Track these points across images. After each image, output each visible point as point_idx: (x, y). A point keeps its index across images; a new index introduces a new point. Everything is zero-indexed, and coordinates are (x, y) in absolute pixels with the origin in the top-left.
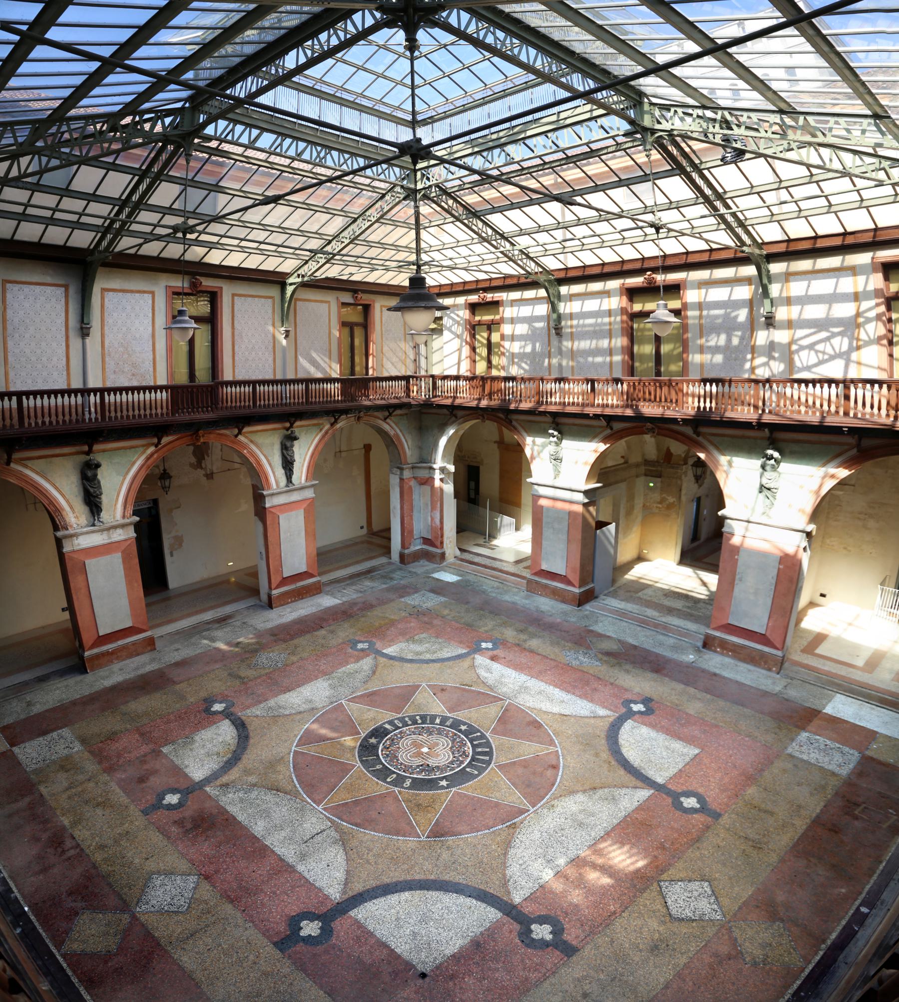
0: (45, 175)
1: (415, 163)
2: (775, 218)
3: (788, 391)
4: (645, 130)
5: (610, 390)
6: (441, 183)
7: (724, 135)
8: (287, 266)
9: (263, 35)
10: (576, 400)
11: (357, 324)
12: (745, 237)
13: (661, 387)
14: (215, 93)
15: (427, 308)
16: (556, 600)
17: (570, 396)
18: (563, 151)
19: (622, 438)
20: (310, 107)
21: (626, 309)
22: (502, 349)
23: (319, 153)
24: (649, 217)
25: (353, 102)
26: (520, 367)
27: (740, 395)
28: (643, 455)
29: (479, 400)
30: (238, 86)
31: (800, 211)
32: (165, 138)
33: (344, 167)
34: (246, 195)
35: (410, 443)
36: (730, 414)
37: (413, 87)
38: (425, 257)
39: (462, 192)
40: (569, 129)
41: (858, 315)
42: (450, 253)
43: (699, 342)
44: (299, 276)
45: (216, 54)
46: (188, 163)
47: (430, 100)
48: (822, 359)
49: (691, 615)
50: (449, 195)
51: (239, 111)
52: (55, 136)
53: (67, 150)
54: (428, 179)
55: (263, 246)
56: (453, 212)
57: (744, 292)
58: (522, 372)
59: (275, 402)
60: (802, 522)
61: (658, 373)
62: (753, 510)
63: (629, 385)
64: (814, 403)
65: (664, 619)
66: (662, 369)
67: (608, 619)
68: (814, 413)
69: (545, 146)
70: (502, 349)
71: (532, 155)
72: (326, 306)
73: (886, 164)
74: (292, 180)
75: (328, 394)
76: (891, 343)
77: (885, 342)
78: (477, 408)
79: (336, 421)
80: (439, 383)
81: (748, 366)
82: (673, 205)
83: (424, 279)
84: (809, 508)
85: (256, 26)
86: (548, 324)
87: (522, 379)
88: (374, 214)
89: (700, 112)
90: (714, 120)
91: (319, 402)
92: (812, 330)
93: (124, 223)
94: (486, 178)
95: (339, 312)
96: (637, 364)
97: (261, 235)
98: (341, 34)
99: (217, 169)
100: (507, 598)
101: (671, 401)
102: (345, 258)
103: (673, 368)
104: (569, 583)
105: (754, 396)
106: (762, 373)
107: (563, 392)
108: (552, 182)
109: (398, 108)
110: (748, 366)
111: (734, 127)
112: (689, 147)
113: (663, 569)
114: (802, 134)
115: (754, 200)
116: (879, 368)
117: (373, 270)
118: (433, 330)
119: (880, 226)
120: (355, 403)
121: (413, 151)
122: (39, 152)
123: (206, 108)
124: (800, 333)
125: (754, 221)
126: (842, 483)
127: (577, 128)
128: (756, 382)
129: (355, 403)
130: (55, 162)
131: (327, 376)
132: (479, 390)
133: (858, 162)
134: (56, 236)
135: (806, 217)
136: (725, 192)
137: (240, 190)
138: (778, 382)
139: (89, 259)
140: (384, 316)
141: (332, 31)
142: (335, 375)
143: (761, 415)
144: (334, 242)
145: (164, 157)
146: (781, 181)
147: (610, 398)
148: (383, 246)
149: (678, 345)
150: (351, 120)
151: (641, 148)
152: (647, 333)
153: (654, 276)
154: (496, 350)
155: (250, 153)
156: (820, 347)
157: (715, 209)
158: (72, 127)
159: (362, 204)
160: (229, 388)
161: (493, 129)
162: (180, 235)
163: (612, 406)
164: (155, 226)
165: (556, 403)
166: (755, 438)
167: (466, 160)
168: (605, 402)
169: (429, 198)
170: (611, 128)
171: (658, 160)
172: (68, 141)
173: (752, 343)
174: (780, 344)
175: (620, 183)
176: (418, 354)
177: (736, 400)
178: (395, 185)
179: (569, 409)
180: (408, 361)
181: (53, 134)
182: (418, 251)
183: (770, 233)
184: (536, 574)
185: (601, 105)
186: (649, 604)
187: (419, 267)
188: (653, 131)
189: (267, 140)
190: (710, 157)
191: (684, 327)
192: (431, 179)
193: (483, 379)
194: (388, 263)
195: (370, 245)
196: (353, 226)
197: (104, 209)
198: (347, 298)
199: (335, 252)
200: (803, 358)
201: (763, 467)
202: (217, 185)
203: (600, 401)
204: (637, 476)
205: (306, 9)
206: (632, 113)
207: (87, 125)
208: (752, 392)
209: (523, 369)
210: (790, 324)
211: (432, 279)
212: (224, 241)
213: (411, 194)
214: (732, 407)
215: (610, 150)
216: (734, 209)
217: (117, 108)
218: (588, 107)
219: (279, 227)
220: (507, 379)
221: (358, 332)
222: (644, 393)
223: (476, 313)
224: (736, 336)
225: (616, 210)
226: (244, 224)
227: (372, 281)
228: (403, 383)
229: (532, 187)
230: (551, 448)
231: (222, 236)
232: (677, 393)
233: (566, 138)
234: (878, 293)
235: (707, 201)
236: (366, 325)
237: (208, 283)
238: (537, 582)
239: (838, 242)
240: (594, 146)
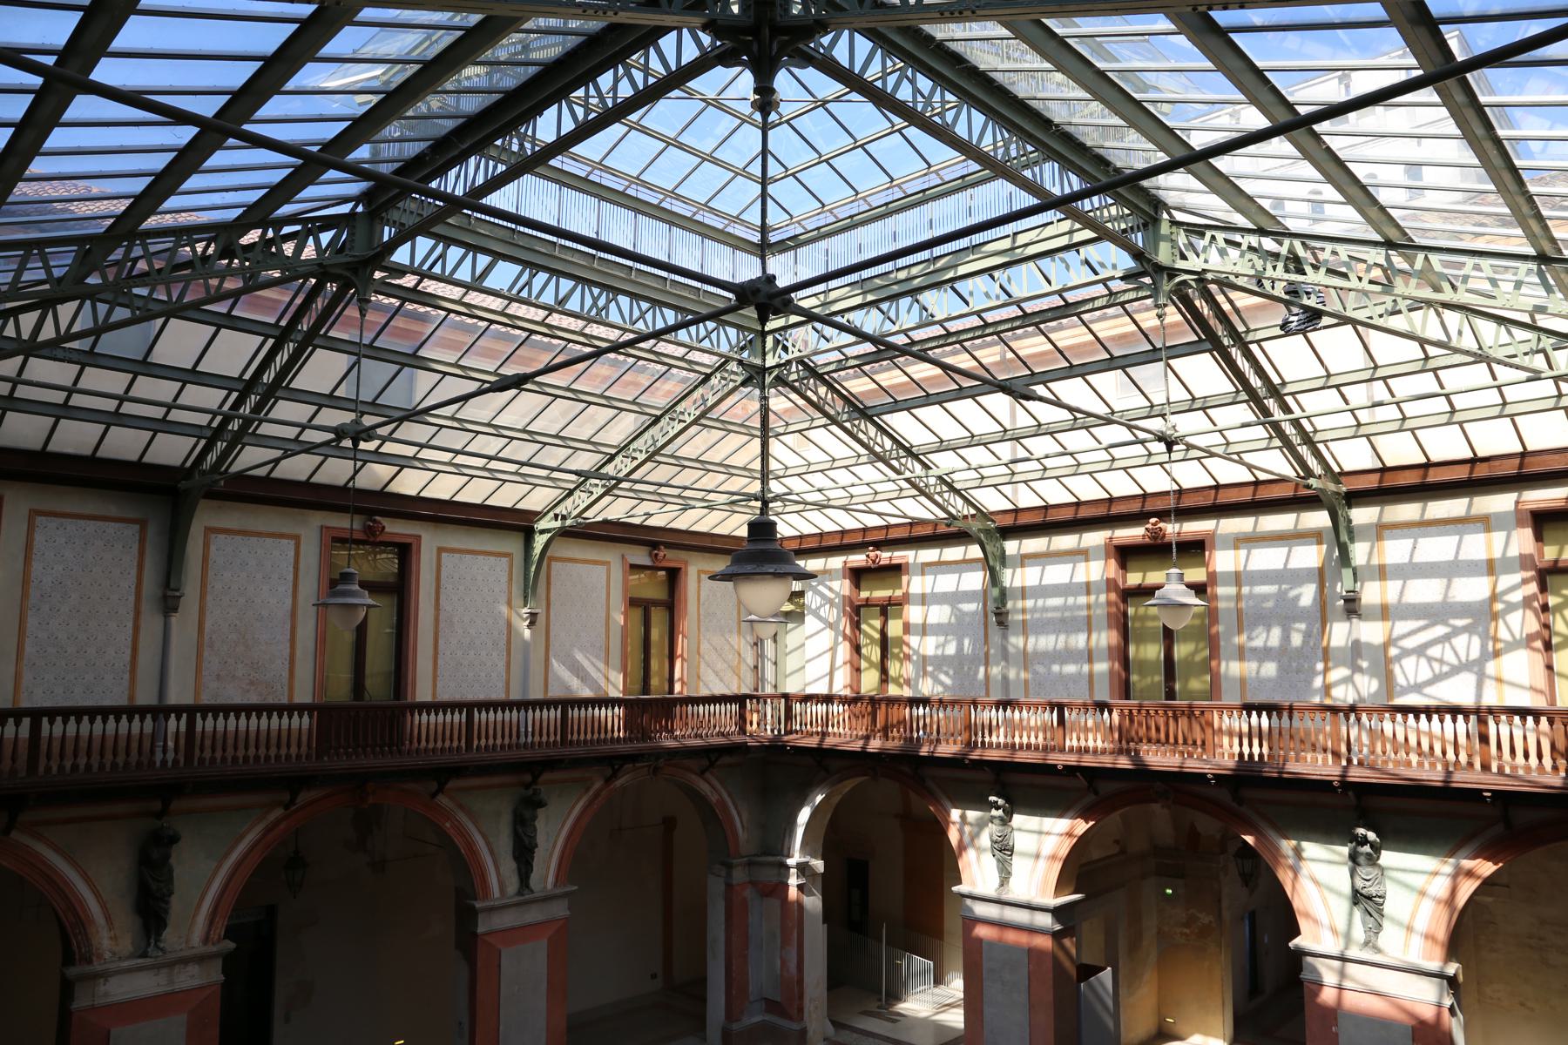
0: (104, 337)
1: (763, 320)
2: (1363, 430)
3: (1388, 726)
4: (1159, 269)
5: (1090, 723)
6: (808, 356)
7: (1291, 283)
8: (537, 500)
9: (497, 76)
10: (1033, 740)
11: (656, 603)
12: (1312, 463)
13: (1176, 719)
14: (408, 187)
15: (778, 576)
17: (1021, 734)
18: (1018, 303)
20: (581, 215)
21: (1115, 581)
22: (905, 649)
23: (595, 300)
24: (1156, 424)
25: (657, 207)
26: (937, 681)
27: (1308, 733)
29: (867, 738)
30: (452, 173)
31: (1404, 419)
32: (322, 271)
33: (640, 325)
34: (465, 373)
35: (745, 816)
36: (1294, 767)
37: (764, 181)
38: (775, 487)
39: (842, 373)
40: (1031, 264)
41: (1494, 597)
42: (818, 480)
43: (1236, 640)
44: (556, 516)
45: (410, 113)
46: (363, 315)
47: (793, 206)
48: (1437, 672)
50: (820, 377)
51: (454, 220)
52: (119, 265)
53: (143, 292)
54: (785, 349)
55: (494, 465)
56: (827, 408)
57: (1309, 556)
58: (940, 689)
59: (507, 741)
61: (1171, 695)
63: (1122, 715)
64: (1431, 748)
66: (1177, 687)
68: (1433, 765)
69: (987, 295)
70: (905, 649)
71: (966, 310)
72: (602, 569)
73: (1547, 342)
74: (549, 347)
75: (601, 727)
76: (1548, 646)
77: (1539, 644)
78: (863, 755)
79: (614, 775)
80: (797, 708)
81: (1318, 682)
82: (1198, 404)
83: (774, 524)
85: (482, 58)
86: (985, 605)
87: (941, 701)
88: (690, 409)
89: (1253, 240)
90: (1276, 256)
91: (585, 741)
92: (1421, 623)
93: (247, 422)
94: (885, 350)
95: (625, 582)
96: (1134, 678)
97: (491, 445)
98: (638, 76)
99: (415, 327)
101: (1194, 743)
102: (638, 487)
103: (1196, 684)
105: (1331, 735)
106: (1343, 695)
107: (1011, 726)
108: (998, 358)
109: (737, 219)
110: (1318, 682)
111: (1308, 269)
112: (1231, 302)
114: (1418, 286)
115: (1330, 399)
116: (1532, 688)
117: (686, 508)
118: (787, 614)
119: (1530, 448)
120: (649, 744)
121: (761, 299)
122: (92, 295)
123: (395, 215)
124: (1402, 627)
125: (1329, 435)
126: (1488, 883)
127: (1044, 263)
128: (1334, 710)
129: (649, 744)
130: (121, 313)
131: (601, 695)
132: (867, 720)
133: (1504, 337)
134: (124, 444)
135: (1412, 430)
136: (1284, 384)
137: (456, 365)
138: (1370, 711)
139: (183, 485)
140: (703, 590)
141: (621, 71)
142: (615, 693)
143: (1346, 769)
144: (619, 459)
145: (320, 304)
146: (1376, 367)
147: (1091, 736)
148: (704, 465)
149: (1201, 645)
150: (653, 240)
151: (1149, 301)
152: (1150, 624)
153: (1162, 525)
154: (896, 651)
155: (475, 298)
156: (1434, 651)
157: (1266, 412)
158: (152, 249)
159: (669, 392)
160: (424, 716)
161: (901, 262)
162: (347, 443)
163: (1095, 751)
164: (304, 427)
165: (998, 745)
167: (851, 316)
168: (1083, 744)
169: (786, 384)
170: (1102, 265)
171: (1176, 324)
172: (146, 274)
173: (1325, 643)
174: (1369, 645)
175: (1113, 363)
176: (760, 656)
177: (1302, 741)
178: (728, 360)
179: (1023, 757)
180: (743, 668)
181: (117, 263)
182: (765, 475)
183: (1353, 456)
185: (1088, 223)
187: (765, 503)
188: (1172, 273)
189: (504, 275)
190: (1261, 318)
191: (1212, 615)
192: (790, 349)
193: (874, 701)
194: (711, 496)
195: (681, 463)
196: (654, 431)
197: (212, 397)
198: (640, 556)
199: (621, 475)
200: (1409, 671)
201: (1353, 857)
202: (414, 355)
203: (1075, 743)
205: (574, 24)
206: (1139, 239)
207: (178, 245)
208: (1328, 728)
209: (942, 684)
210: (1385, 612)
211: (789, 526)
212: (426, 454)
213: (755, 376)
214: (1297, 755)
215: (1098, 303)
216: (1297, 413)
217: (234, 214)
218: (1066, 225)
219: (524, 431)
220: (914, 702)
221: (658, 616)
222: (1148, 728)
223: (863, 584)
224: (1298, 630)
225: (1102, 410)
226: (462, 425)
227: (683, 527)
228: (735, 707)
229: (962, 366)
231: (422, 446)
232: (1203, 729)
233: (1024, 282)
234: (1525, 561)
235: (1254, 398)
236: (672, 606)
237: (395, 528)
239: (1462, 473)
240: (1072, 297)
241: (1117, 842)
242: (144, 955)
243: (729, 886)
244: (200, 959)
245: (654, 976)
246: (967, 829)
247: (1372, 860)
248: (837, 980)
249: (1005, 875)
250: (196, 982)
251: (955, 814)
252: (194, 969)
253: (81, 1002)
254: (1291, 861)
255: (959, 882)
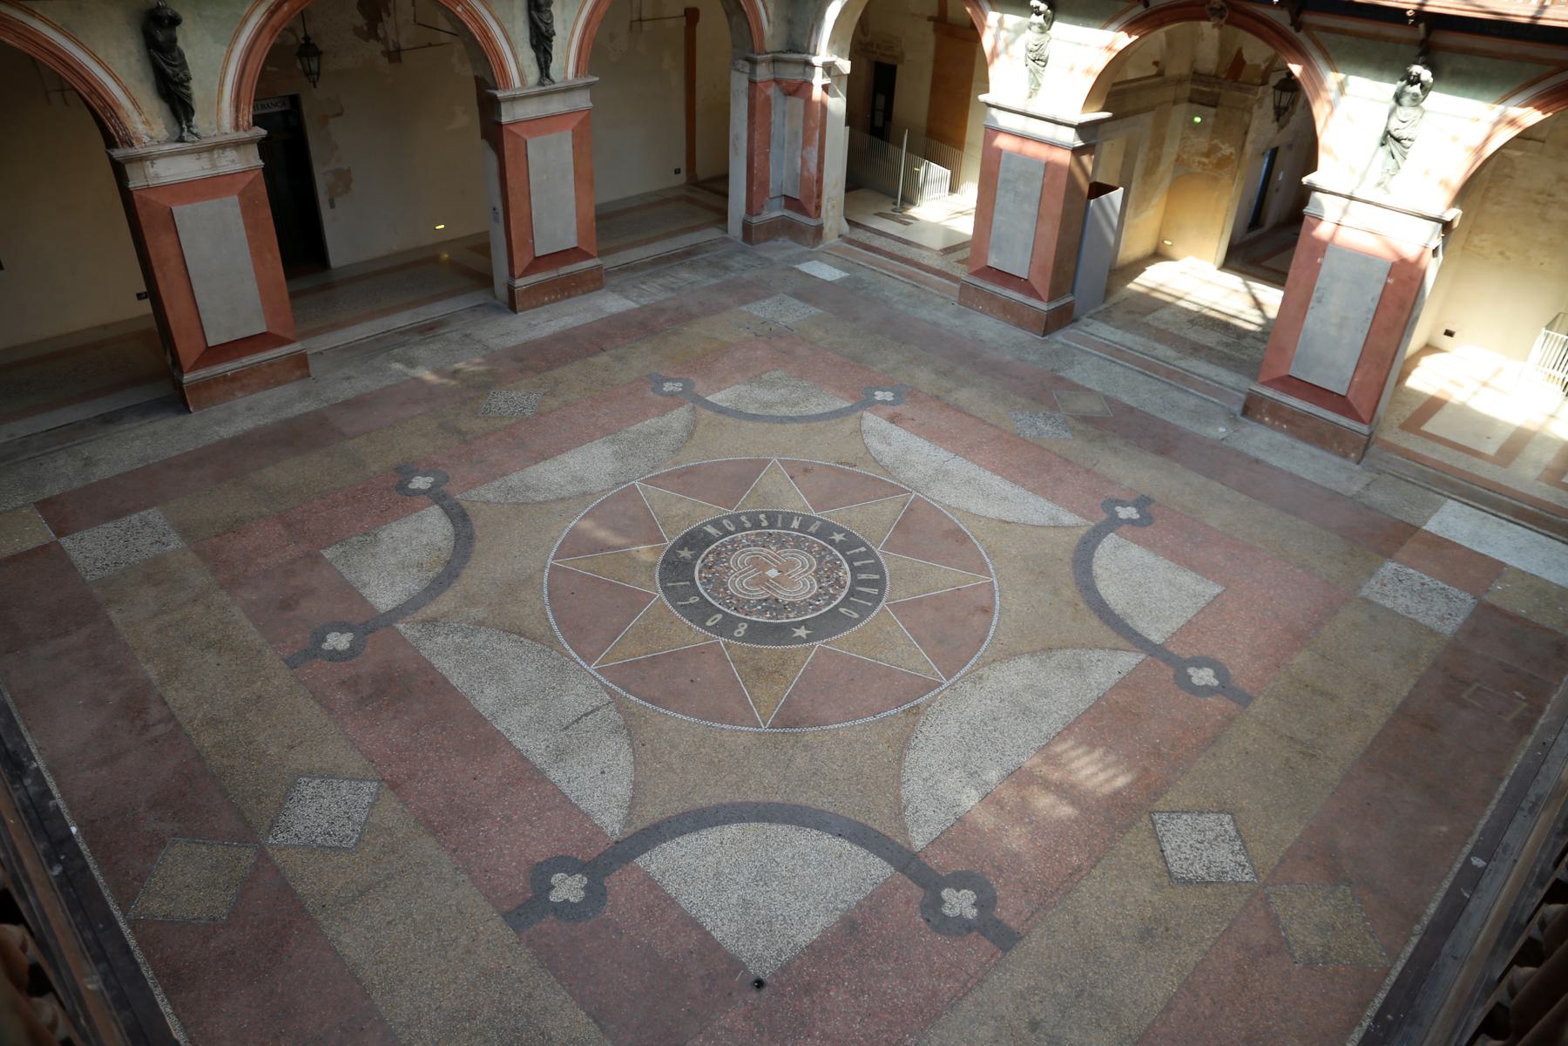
16: (1008, 322)
19: (1161, 24)
28: (1193, 62)
35: (771, 11)
49: (1230, 358)
60: (1441, 204)
62: (1363, 177)
65: (1183, 364)
67: (1092, 360)
84: (1457, 179)
100: (924, 313)
104: (1032, 292)
113: (1196, 276)
126: (1526, 136)
166: (1398, 41)
184: (976, 274)
186: (1162, 336)
201: (1398, 98)
204: (1175, 103)
230: (1031, 37)
238: (978, 289)
241: (1156, 63)
242: (181, 140)
243: (752, 83)
244: (237, 145)
245: (677, 171)
246: (1003, 34)
247: (1416, 101)
248: (854, 183)
249: (1036, 86)
250: (238, 167)
251: (993, 17)
252: (231, 154)
253: (135, 183)
254: (1332, 96)
255: (987, 91)
